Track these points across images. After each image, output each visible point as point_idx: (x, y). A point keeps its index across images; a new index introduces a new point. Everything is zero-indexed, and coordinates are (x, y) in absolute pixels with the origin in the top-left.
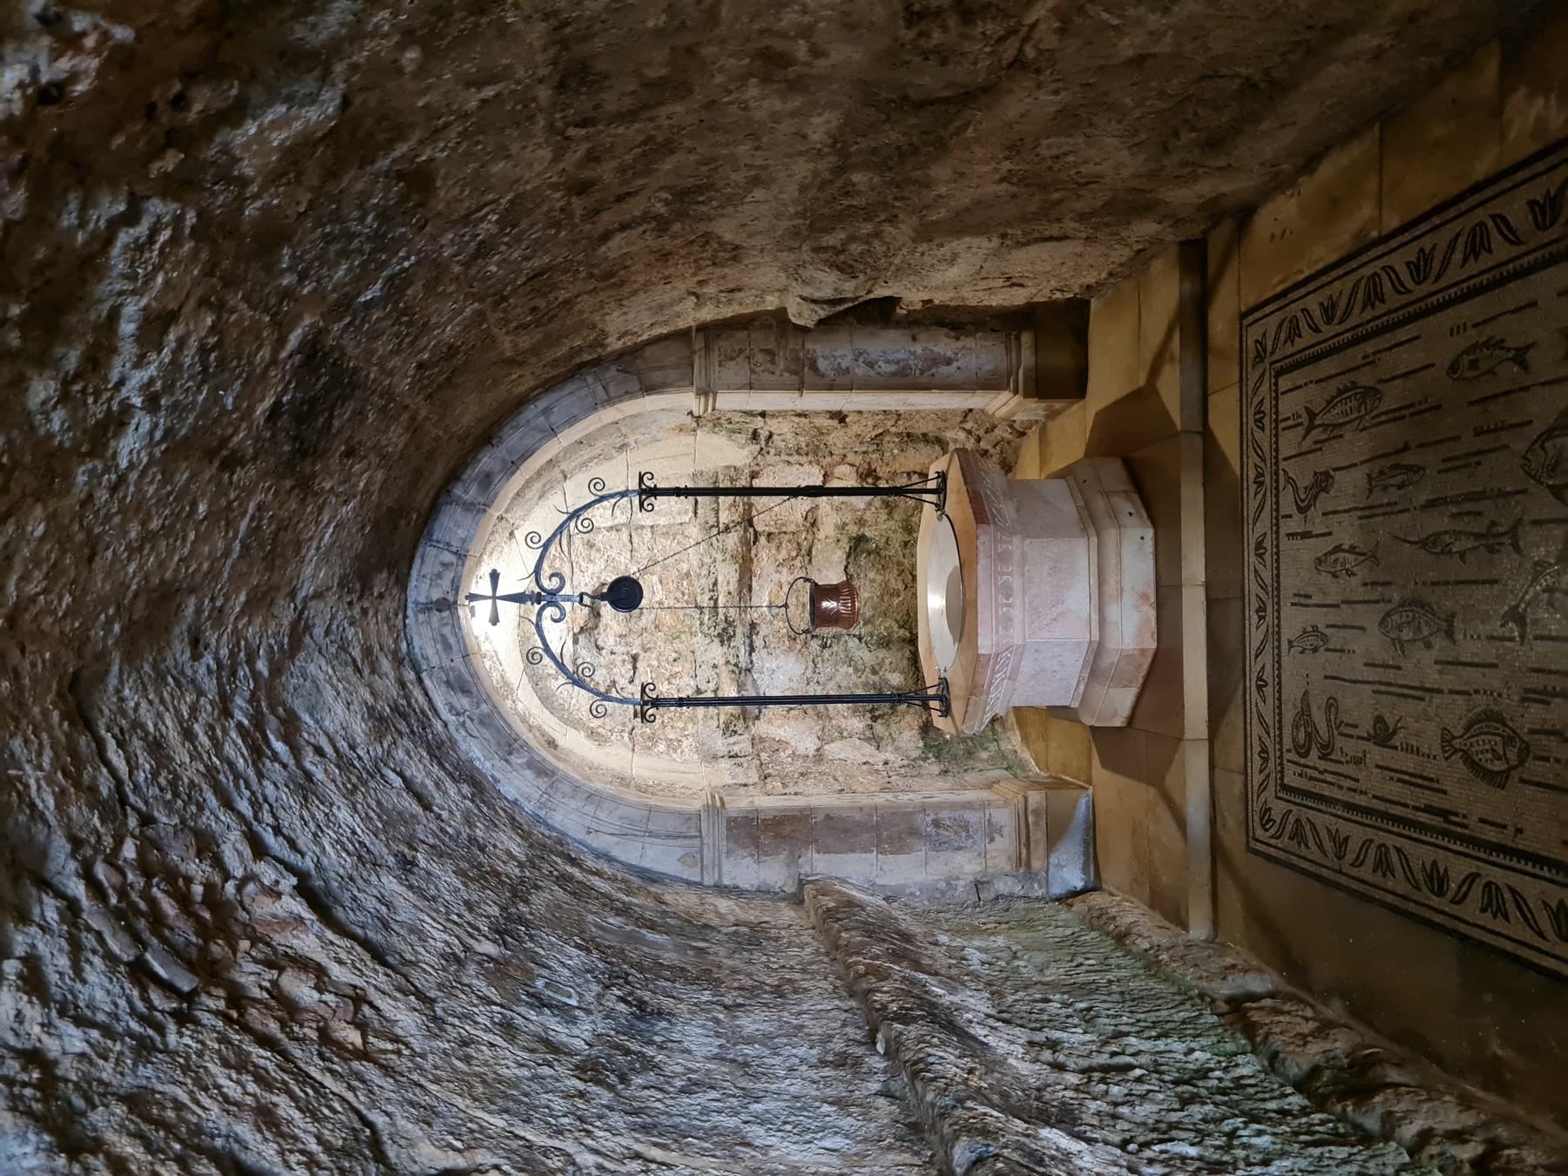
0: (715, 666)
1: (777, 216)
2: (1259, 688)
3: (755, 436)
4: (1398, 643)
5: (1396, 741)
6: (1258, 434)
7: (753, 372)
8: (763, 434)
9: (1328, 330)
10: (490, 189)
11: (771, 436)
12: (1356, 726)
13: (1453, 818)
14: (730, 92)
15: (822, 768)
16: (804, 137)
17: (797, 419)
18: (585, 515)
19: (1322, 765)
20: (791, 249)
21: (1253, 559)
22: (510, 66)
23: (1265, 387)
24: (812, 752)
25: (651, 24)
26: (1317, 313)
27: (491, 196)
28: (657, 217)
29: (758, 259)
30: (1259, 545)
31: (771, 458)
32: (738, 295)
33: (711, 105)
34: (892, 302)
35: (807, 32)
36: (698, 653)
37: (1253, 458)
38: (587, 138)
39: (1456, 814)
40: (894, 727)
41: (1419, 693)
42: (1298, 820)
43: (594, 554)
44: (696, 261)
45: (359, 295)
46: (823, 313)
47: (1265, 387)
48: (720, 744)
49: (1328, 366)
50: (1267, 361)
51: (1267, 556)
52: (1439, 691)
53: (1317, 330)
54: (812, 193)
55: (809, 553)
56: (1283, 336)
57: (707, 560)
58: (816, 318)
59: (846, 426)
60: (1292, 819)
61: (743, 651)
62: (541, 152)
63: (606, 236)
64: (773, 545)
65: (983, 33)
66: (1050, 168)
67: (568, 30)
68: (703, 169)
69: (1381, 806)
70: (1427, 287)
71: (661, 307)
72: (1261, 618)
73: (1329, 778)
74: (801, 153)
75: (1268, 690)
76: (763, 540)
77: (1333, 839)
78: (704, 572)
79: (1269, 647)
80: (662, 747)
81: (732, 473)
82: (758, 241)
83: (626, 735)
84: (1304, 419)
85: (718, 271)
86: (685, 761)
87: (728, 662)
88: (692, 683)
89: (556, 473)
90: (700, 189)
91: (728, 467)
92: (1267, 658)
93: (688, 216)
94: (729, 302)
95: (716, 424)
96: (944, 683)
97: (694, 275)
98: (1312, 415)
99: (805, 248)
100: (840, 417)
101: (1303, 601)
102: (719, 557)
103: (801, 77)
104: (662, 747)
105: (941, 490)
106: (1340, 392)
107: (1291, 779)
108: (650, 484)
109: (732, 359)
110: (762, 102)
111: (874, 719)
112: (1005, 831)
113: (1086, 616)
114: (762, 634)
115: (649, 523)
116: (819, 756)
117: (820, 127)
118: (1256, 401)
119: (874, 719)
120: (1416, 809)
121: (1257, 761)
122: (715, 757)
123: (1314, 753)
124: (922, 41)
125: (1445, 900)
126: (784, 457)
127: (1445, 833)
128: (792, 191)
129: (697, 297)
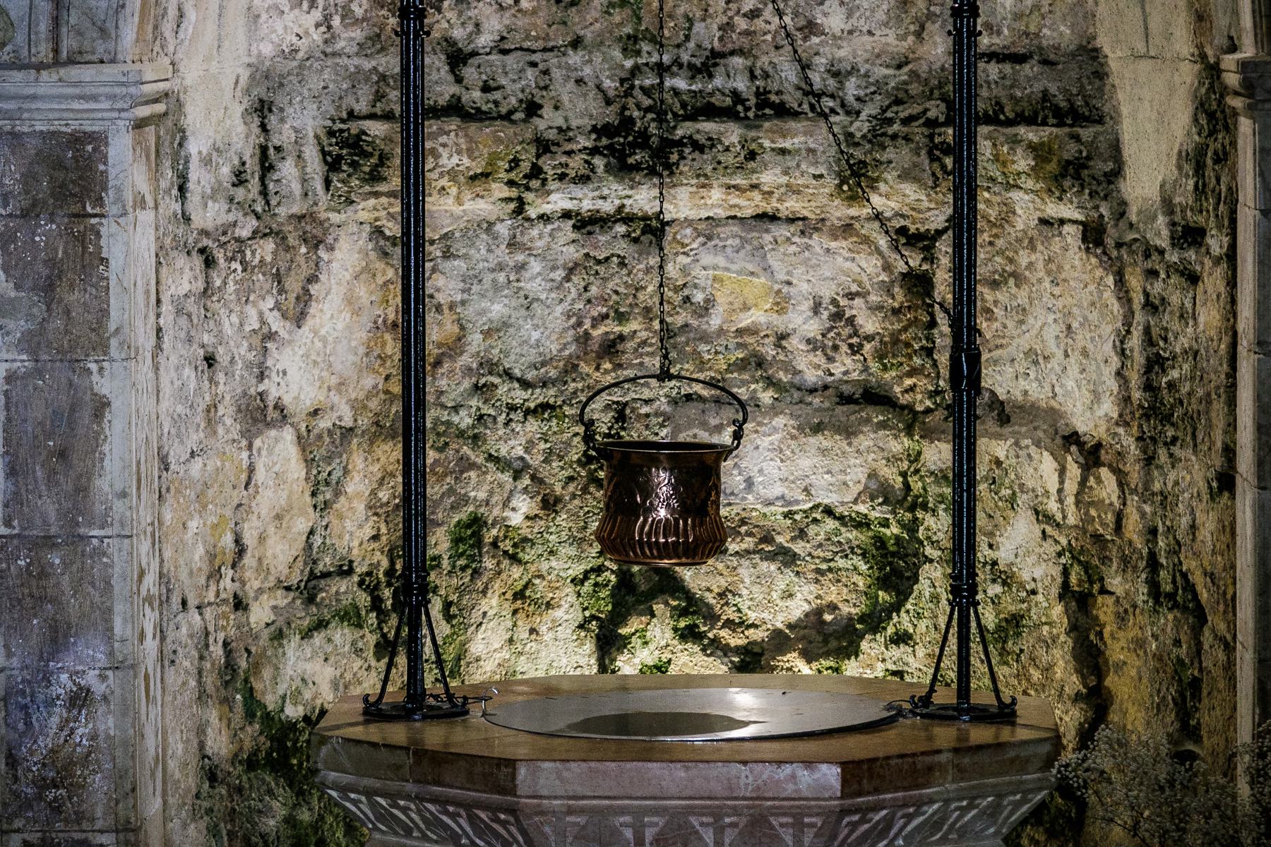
0: (533, 109)
15: (229, 424)
36: (574, 58)
57: (852, 88)
88: (484, 40)
102: (860, 127)
111: (369, 584)
119: (369, 584)
122: (262, 110)
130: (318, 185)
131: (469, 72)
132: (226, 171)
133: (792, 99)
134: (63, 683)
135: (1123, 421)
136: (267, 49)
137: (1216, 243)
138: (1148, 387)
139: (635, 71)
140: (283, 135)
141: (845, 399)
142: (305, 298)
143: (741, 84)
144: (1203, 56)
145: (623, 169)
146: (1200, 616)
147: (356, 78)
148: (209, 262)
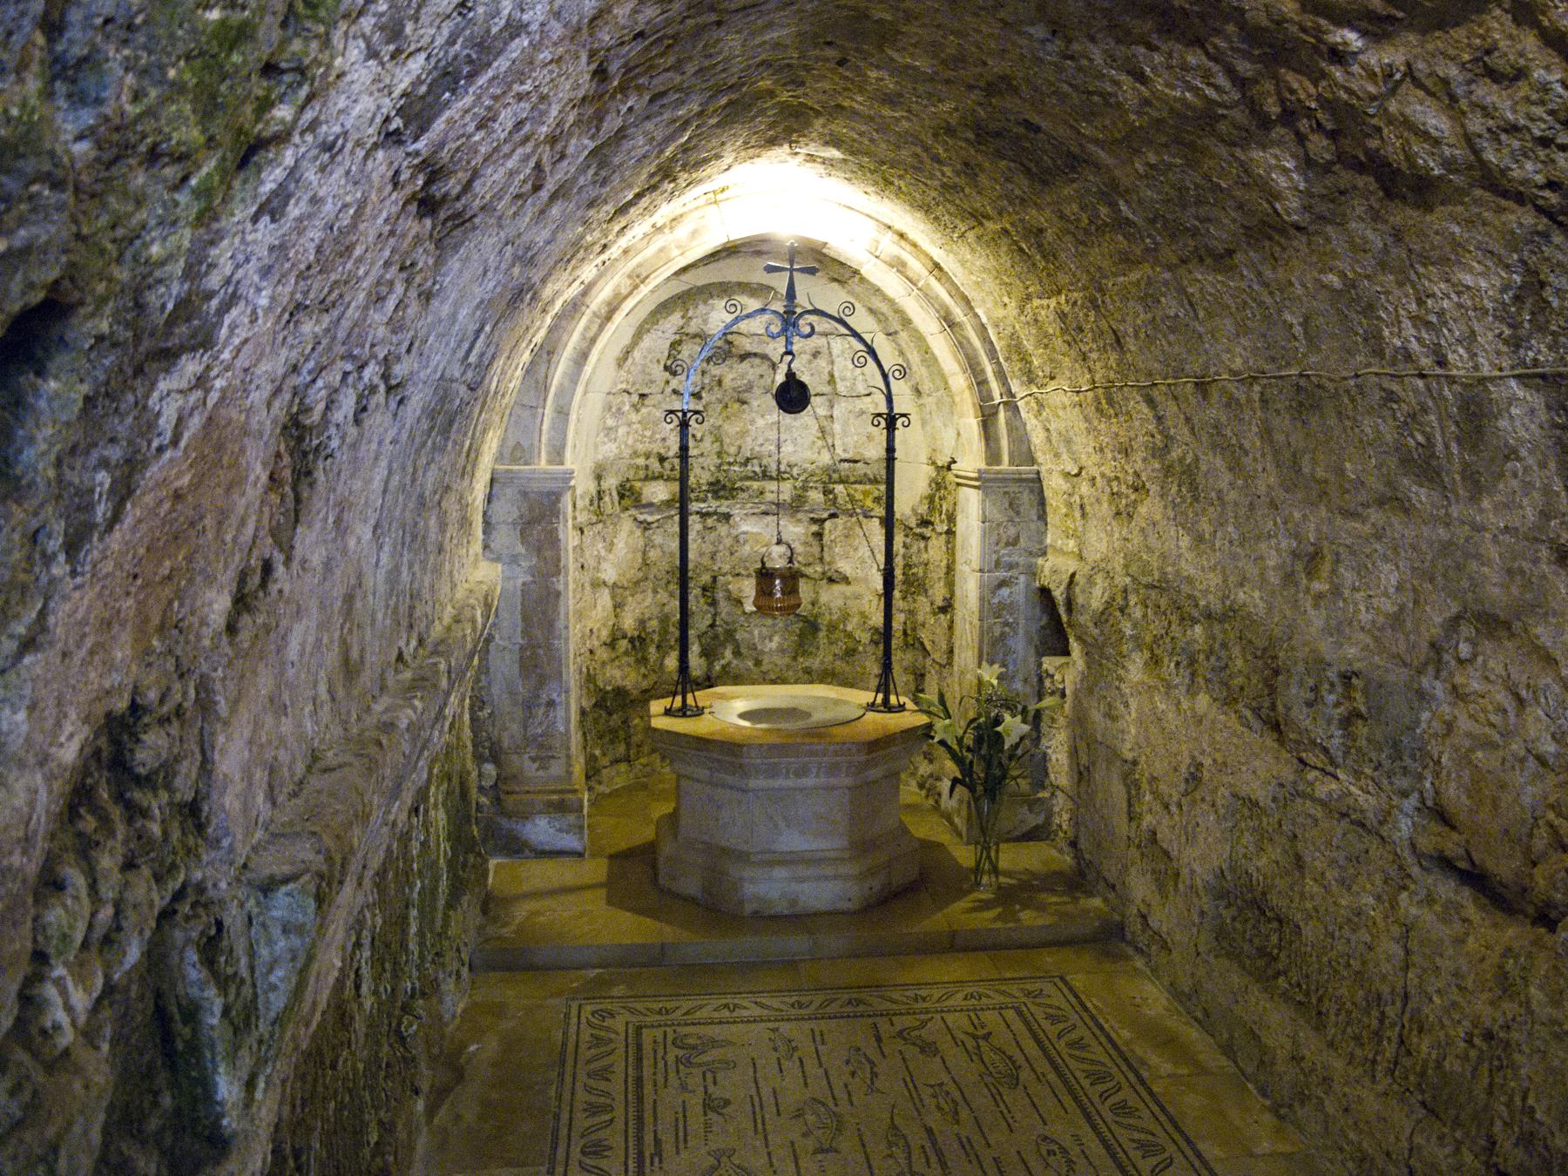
1: (1163, 556)
2: (726, 1006)
3: (925, 523)
4: (799, 1114)
5: (711, 1115)
6: (960, 996)
7: (999, 525)
8: (927, 532)
9: (1061, 1045)
10: (1210, 315)
11: (924, 538)
12: (715, 1083)
13: (656, 1160)
14: (1285, 523)
16: (1242, 585)
18: (870, 360)
19: (671, 1058)
20: (1126, 566)
21: (846, 997)
22: (1319, 350)
23: (1002, 999)
24: (603, 576)
25: (1348, 465)
26: (1074, 1036)
27: (1201, 314)
28: (1166, 448)
29: (1117, 535)
30: (859, 1002)
32: (1078, 514)
33: (1273, 505)
35: (1336, 591)
36: (701, 460)
37: (937, 994)
38: (1249, 400)
39: (661, 1161)
41: (760, 1126)
42: (611, 1040)
44: (1117, 478)
45: (1127, 201)
46: (1058, 594)
47: (1002, 999)
48: (611, 482)
50: (1028, 1001)
51: (849, 1009)
52: (767, 1146)
53: (1059, 1036)
54: (1185, 588)
56: (1049, 1011)
57: (795, 471)
58: (1052, 587)
60: (613, 1036)
62: (1239, 361)
63: (1150, 402)
64: (810, 539)
65: (1331, 736)
66: (1203, 800)
67: (1346, 400)
68: (1213, 494)
69: (648, 1106)
70: (1109, 1116)
71: (1069, 442)
72: (793, 1005)
73: (661, 1065)
74: (1225, 581)
75: (726, 1013)
76: (815, 528)
77: (605, 1069)
79: (766, 1012)
82: (1137, 539)
83: (624, 386)
84: (981, 1032)
85: (1105, 498)
86: (596, 446)
89: (896, 326)
90: (1193, 487)
92: (757, 1012)
93: (1166, 476)
94: (1069, 505)
95: (938, 485)
96: (699, 712)
97: (1103, 475)
98: (987, 1037)
99: (1128, 580)
100: (946, 608)
101: (818, 1038)
102: (799, 484)
103: (1296, 584)
104: (610, 422)
105: (887, 707)
106: (1010, 1058)
107: (647, 1035)
108: (899, 423)
109: (1011, 504)
112: (540, 773)
113: (773, 847)
115: (836, 413)
116: (597, 584)
117: (1251, 598)
118: (991, 993)
119: (632, 640)
120: (655, 1132)
121: (656, 1006)
122: (599, 478)
123: (681, 1053)
124: (1327, 686)
125: (579, 1156)
127: (640, 1155)
128: (1188, 569)
129: (1077, 475)
131: (667, 465)
133: (774, 474)
134: (544, 697)
140: (605, 485)
142: (612, 544)
143: (757, 469)
144: (934, 463)
145: (717, 497)
146: (926, 653)
147: (630, 467)
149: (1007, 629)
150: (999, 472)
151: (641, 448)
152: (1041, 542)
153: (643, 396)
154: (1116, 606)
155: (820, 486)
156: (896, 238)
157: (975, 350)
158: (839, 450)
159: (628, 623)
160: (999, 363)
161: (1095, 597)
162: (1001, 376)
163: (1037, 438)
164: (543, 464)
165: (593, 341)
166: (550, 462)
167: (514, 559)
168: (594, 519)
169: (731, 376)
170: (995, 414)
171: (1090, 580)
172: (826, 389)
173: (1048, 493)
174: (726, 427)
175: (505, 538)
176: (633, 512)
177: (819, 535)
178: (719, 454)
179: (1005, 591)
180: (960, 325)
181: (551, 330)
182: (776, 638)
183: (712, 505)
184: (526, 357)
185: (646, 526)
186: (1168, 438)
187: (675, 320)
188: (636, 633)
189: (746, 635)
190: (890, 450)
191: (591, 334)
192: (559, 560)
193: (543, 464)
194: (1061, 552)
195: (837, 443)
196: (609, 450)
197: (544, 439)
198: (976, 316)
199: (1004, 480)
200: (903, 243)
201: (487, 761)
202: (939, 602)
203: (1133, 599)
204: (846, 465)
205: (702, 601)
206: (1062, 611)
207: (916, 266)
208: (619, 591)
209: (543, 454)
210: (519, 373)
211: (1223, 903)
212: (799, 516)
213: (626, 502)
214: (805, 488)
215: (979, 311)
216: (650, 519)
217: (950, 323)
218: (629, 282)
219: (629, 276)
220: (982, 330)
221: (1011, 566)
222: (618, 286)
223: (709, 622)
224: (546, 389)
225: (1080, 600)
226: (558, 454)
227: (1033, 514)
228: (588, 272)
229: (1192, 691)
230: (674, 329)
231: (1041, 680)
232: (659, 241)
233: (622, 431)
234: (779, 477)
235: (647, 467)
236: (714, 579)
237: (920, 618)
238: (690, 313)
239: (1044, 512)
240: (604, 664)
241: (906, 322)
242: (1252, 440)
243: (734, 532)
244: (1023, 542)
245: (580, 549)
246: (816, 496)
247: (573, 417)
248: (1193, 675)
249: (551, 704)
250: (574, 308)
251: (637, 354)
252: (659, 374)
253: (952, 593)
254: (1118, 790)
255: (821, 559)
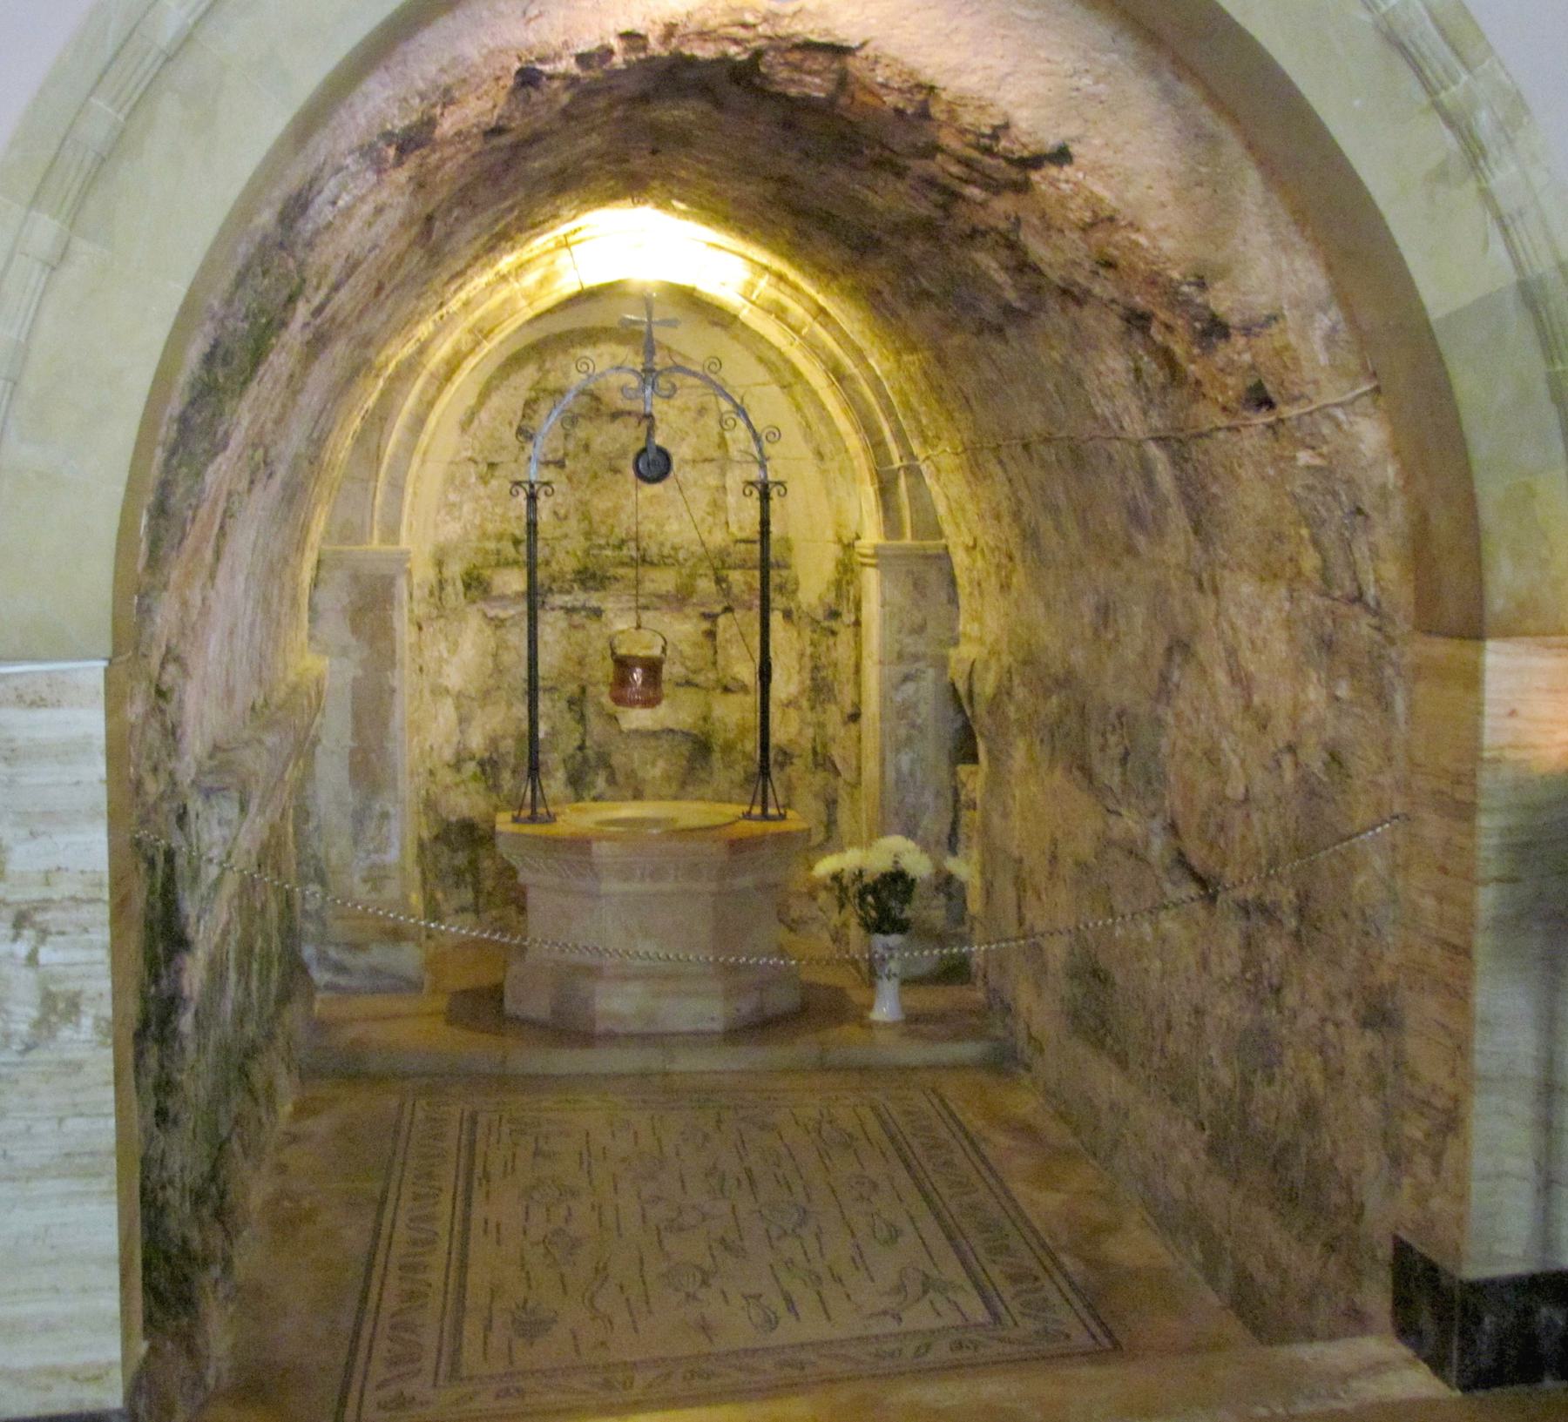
8: (834, 624)
15: (427, 695)
17: (852, 662)
24: (446, 682)
31: (807, 634)
34: (973, 758)
36: (565, 543)
40: (472, 786)
43: (690, 415)
46: (962, 687)
48: (455, 570)
49: (873, 1126)
55: (689, 683)
59: (845, 724)
61: (567, 600)
64: (701, 639)
71: (963, 510)
76: (706, 625)
78: (666, 551)
80: (453, 497)
81: (790, 587)
83: (469, 454)
85: (992, 570)
86: (436, 526)
87: (554, 580)
89: (789, 378)
91: (797, 583)
94: (970, 582)
100: (855, 717)
102: (685, 571)
104: (453, 497)
105: (765, 816)
108: (774, 493)
109: (915, 585)
110: (1087, 607)
114: (588, 623)
115: (729, 483)
116: (439, 691)
117: (1078, 657)
119: (481, 764)
122: (440, 564)
126: (809, 650)
129: (974, 547)
130: (461, 596)
132: (426, 591)
135: (802, 693)
136: (442, 539)
137: (848, 618)
138: (813, 679)
139: (590, 547)
140: (447, 573)
141: (678, 685)
142: (456, 644)
143: (634, 553)
144: (840, 540)
145: (585, 589)
146: (837, 773)
147: (477, 551)
148: (420, 628)
149: (914, 732)
150: (900, 548)
151: (490, 527)
152: (953, 629)
153: (492, 466)
154: (1004, 692)
155: (710, 573)
156: (774, 280)
157: (869, 406)
158: (734, 529)
159: (476, 741)
160: (897, 421)
161: (987, 686)
162: (900, 436)
163: (942, 508)
164: (375, 544)
165: (431, 404)
166: (383, 541)
167: (344, 651)
168: (435, 613)
169: (599, 440)
170: (896, 478)
171: (987, 667)
172: (716, 454)
173: (957, 572)
174: (595, 501)
175: (335, 628)
176: (481, 605)
177: (711, 635)
178: (588, 535)
179: (910, 687)
180: (852, 379)
181: (384, 394)
182: (661, 764)
183: (579, 597)
184: (356, 423)
185: (498, 624)
186: (1020, 502)
187: (530, 373)
188: (487, 755)
189: (624, 759)
190: (765, 523)
191: (428, 397)
192: (394, 651)
193: (375, 544)
194: (970, 639)
195: (732, 518)
196: (452, 530)
197: (377, 517)
198: (869, 366)
199: (904, 555)
200: (782, 286)
201: (312, 881)
202: (849, 710)
203: (1016, 680)
204: (742, 547)
205: (568, 716)
206: (965, 702)
207: (797, 311)
208: (464, 701)
209: (376, 533)
210: (349, 442)
211: (1076, 982)
212: (688, 610)
213: (474, 593)
214: (693, 576)
215: (872, 362)
216: (502, 614)
217: (838, 375)
218: (470, 337)
219: (471, 331)
220: (876, 384)
221: (916, 658)
222: (459, 341)
223: (577, 743)
224: (379, 459)
225: (977, 688)
226: (392, 532)
227: (943, 596)
228: (424, 330)
229: (1051, 768)
230: (528, 384)
231: (956, 793)
232: (504, 292)
233: (467, 508)
234: (664, 562)
235: (498, 552)
236: (583, 690)
237: (830, 730)
238: (548, 365)
239: (955, 593)
240: (447, 788)
241: (797, 374)
242: (1062, 501)
243: (607, 632)
244: (931, 629)
245: (418, 648)
246: (706, 585)
247: (409, 490)
248: (1054, 748)
249: (385, 816)
250: (410, 368)
251: (484, 415)
252: (509, 435)
253: (859, 695)
254: (1011, 893)
255: (715, 663)
